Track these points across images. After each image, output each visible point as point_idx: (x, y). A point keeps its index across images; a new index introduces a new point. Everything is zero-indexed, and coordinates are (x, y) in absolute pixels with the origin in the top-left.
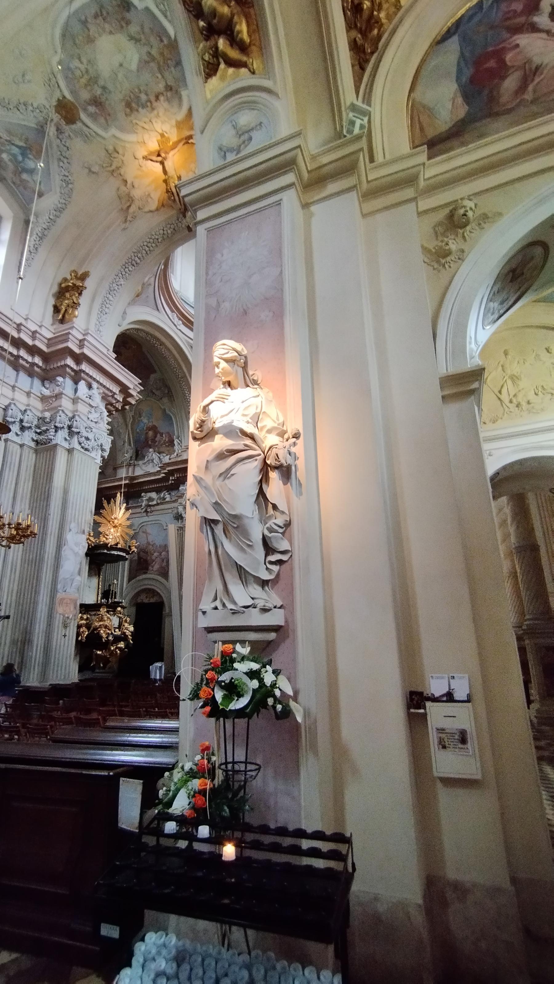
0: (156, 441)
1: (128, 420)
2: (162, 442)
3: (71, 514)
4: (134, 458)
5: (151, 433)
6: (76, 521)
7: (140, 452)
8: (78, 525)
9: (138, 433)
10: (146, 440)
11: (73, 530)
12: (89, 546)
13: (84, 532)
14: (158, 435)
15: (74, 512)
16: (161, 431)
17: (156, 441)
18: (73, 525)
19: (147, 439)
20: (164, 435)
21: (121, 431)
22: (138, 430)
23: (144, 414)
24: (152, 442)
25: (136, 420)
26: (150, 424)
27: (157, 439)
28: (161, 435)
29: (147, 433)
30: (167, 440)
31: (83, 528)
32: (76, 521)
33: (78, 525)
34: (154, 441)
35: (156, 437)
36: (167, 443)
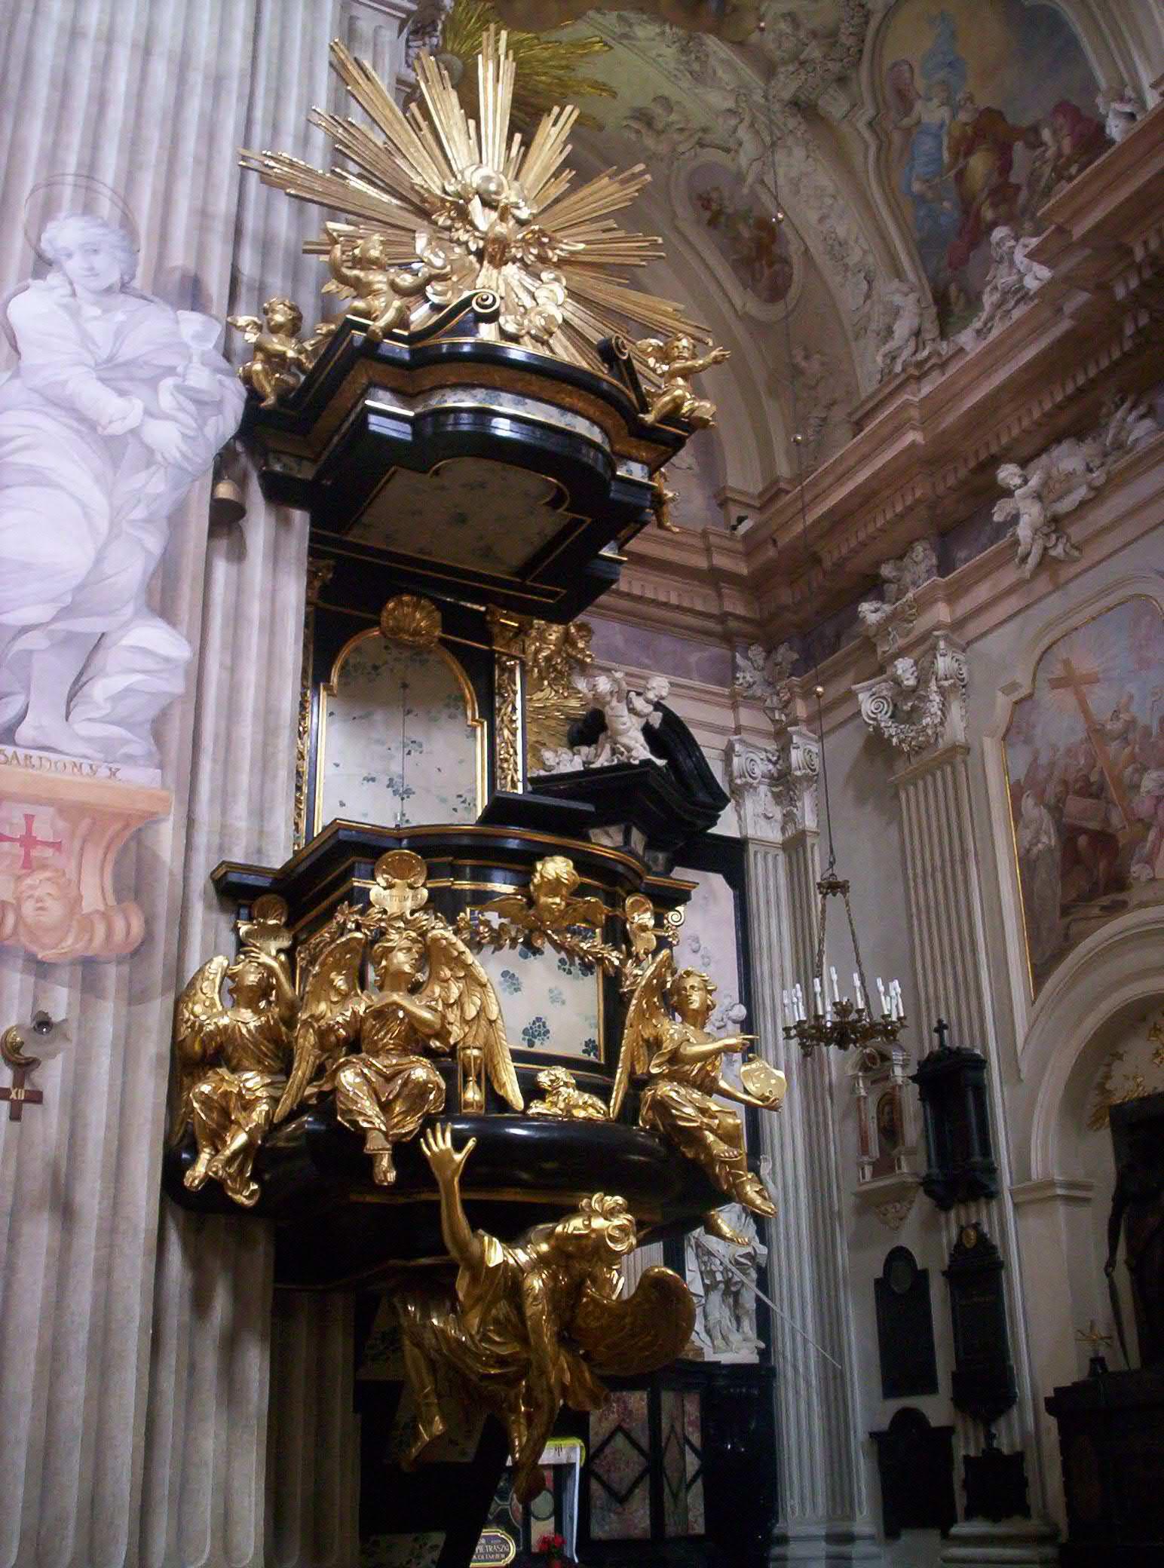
0: (1018, 188)
1: (858, 160)
2: (1047, 170)
3: (52, 157)
4: (931, 330)
5: (979, 164)
6: (106, 206)
7: (953, 290)
8: (127, 223)
9: (920, 199)
10: (966, 212)
11: (75, 266)
12: (254, 396)
13: (192, 294)
14: (1019, 147)
15: (75, 139)
16: (1025, 122)
17: (1018, 188)
18: (66, 233)
19: (967, 205)
20: (1046, 134)
21: (841, 232)
22: (917, 187)
23: (920, 84)
24: (994, 205)
25: (897, 138)
26: (963, 117)
27: (1017, 176)
28: (1032, 136)
29: (960, 177)
30: (1067, 149)
31: (179, 257)
32: (106, 206)
33: (127, 223)
34: (1002, 192)
35: (1005, 166)
36: (1070, 161)
